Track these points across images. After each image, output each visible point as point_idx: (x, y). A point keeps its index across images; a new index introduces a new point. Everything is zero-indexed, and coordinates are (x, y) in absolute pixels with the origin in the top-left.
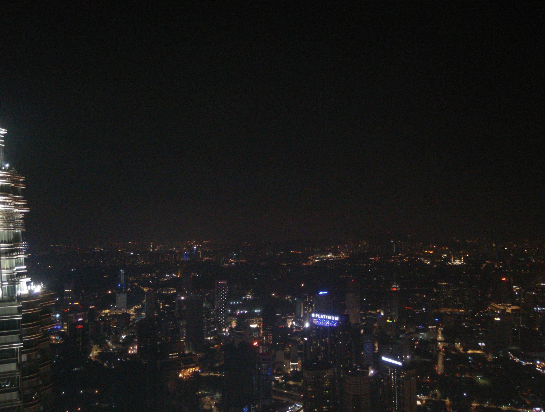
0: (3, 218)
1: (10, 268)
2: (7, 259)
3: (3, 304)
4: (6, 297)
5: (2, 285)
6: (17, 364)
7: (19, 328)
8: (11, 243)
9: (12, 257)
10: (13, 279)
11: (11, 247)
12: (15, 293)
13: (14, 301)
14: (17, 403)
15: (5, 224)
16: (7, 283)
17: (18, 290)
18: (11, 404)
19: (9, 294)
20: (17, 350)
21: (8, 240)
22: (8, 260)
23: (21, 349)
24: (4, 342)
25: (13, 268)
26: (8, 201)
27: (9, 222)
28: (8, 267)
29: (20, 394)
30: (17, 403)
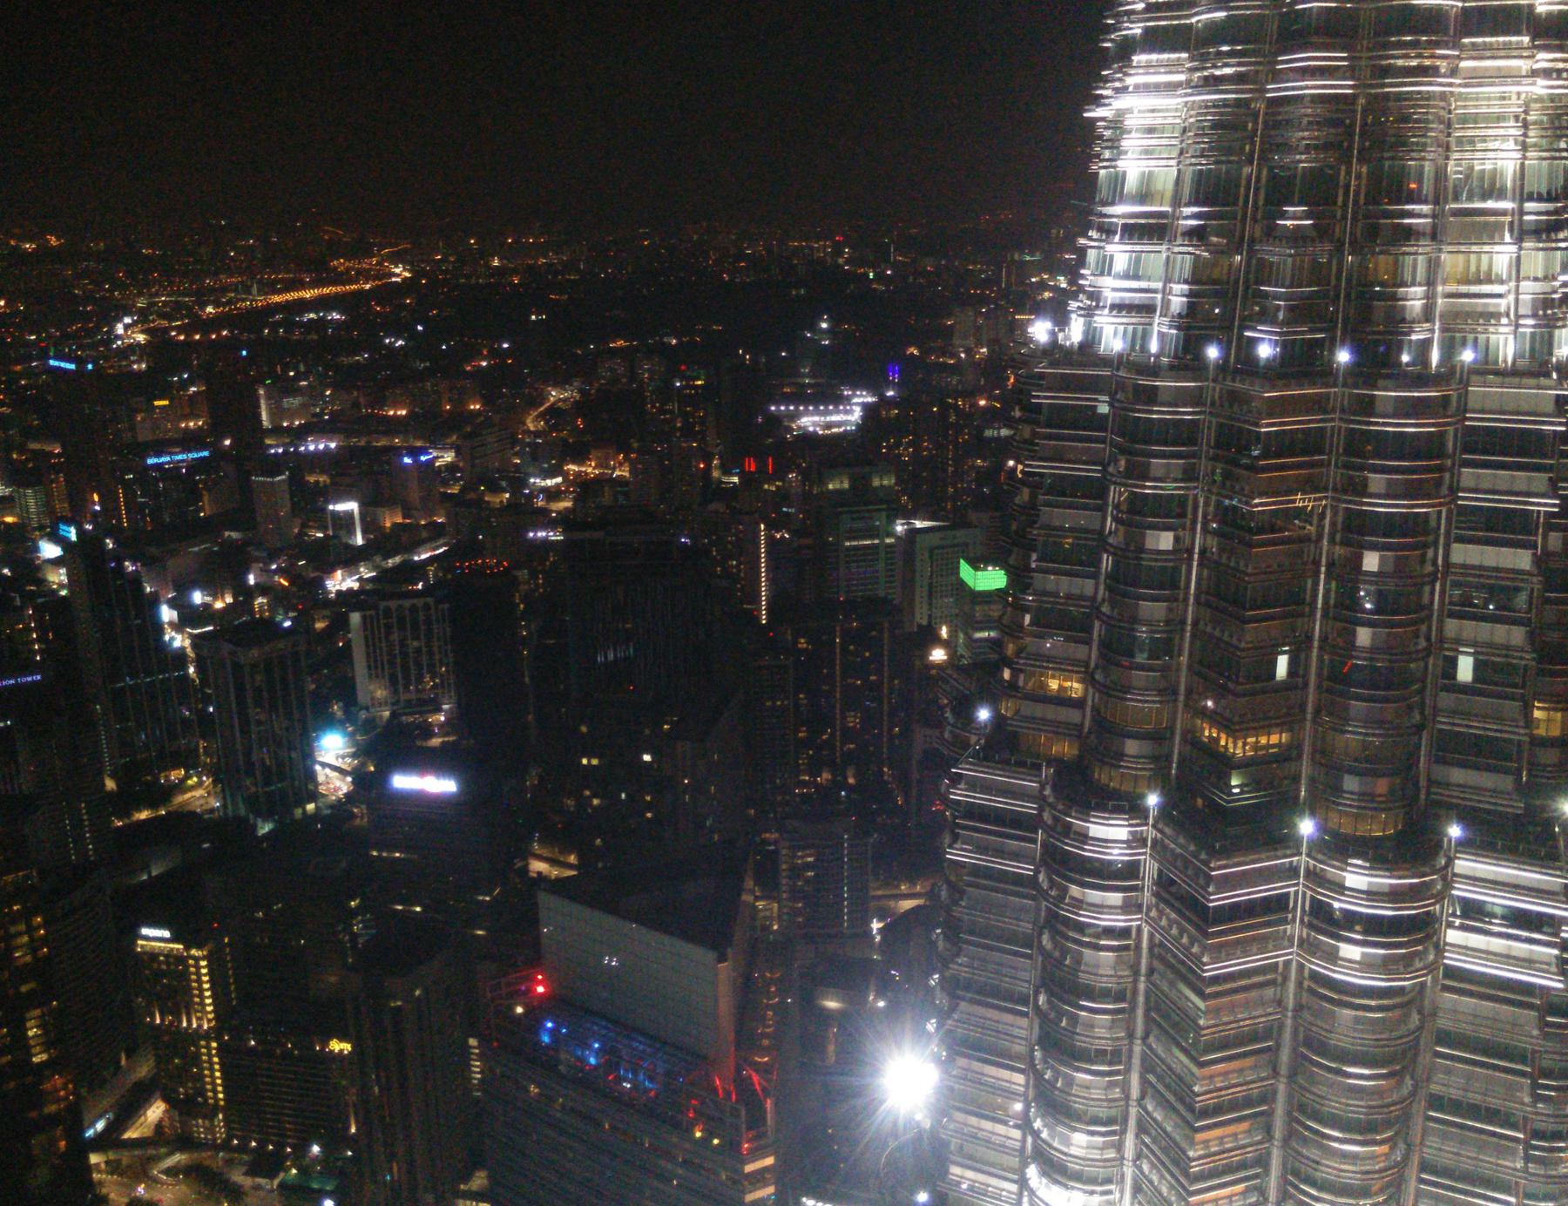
0: (1542, 122)
1: (1545, 278)
2: (1542, 249)
3: (1516, 380)
4: (1523, 363)
5: (1517, 326)
6: (1534, 555)
7: (1552, 458)
8: (1556, 200)
9: (1554, 245)
10: (1549, 312)
11: (1556, 212)
12: (1551, 354)
13: (1548, 375)
14: (1521, 658)
15: (1544, 141)
16: (1531, 322)
17: (1560, 348)
18: (1507, 656)
19: (1532, 356)
20: (1538, 517)
21: (1549, 193)
22: (1541, 253)
23: (1553, 515)
24: (1504, 487)
25: (1554, 278)
26: (1561, 65)
27: (1558, 132)
28: (1540, 275)
29: (1531, 636)
30: (1521, 658)
